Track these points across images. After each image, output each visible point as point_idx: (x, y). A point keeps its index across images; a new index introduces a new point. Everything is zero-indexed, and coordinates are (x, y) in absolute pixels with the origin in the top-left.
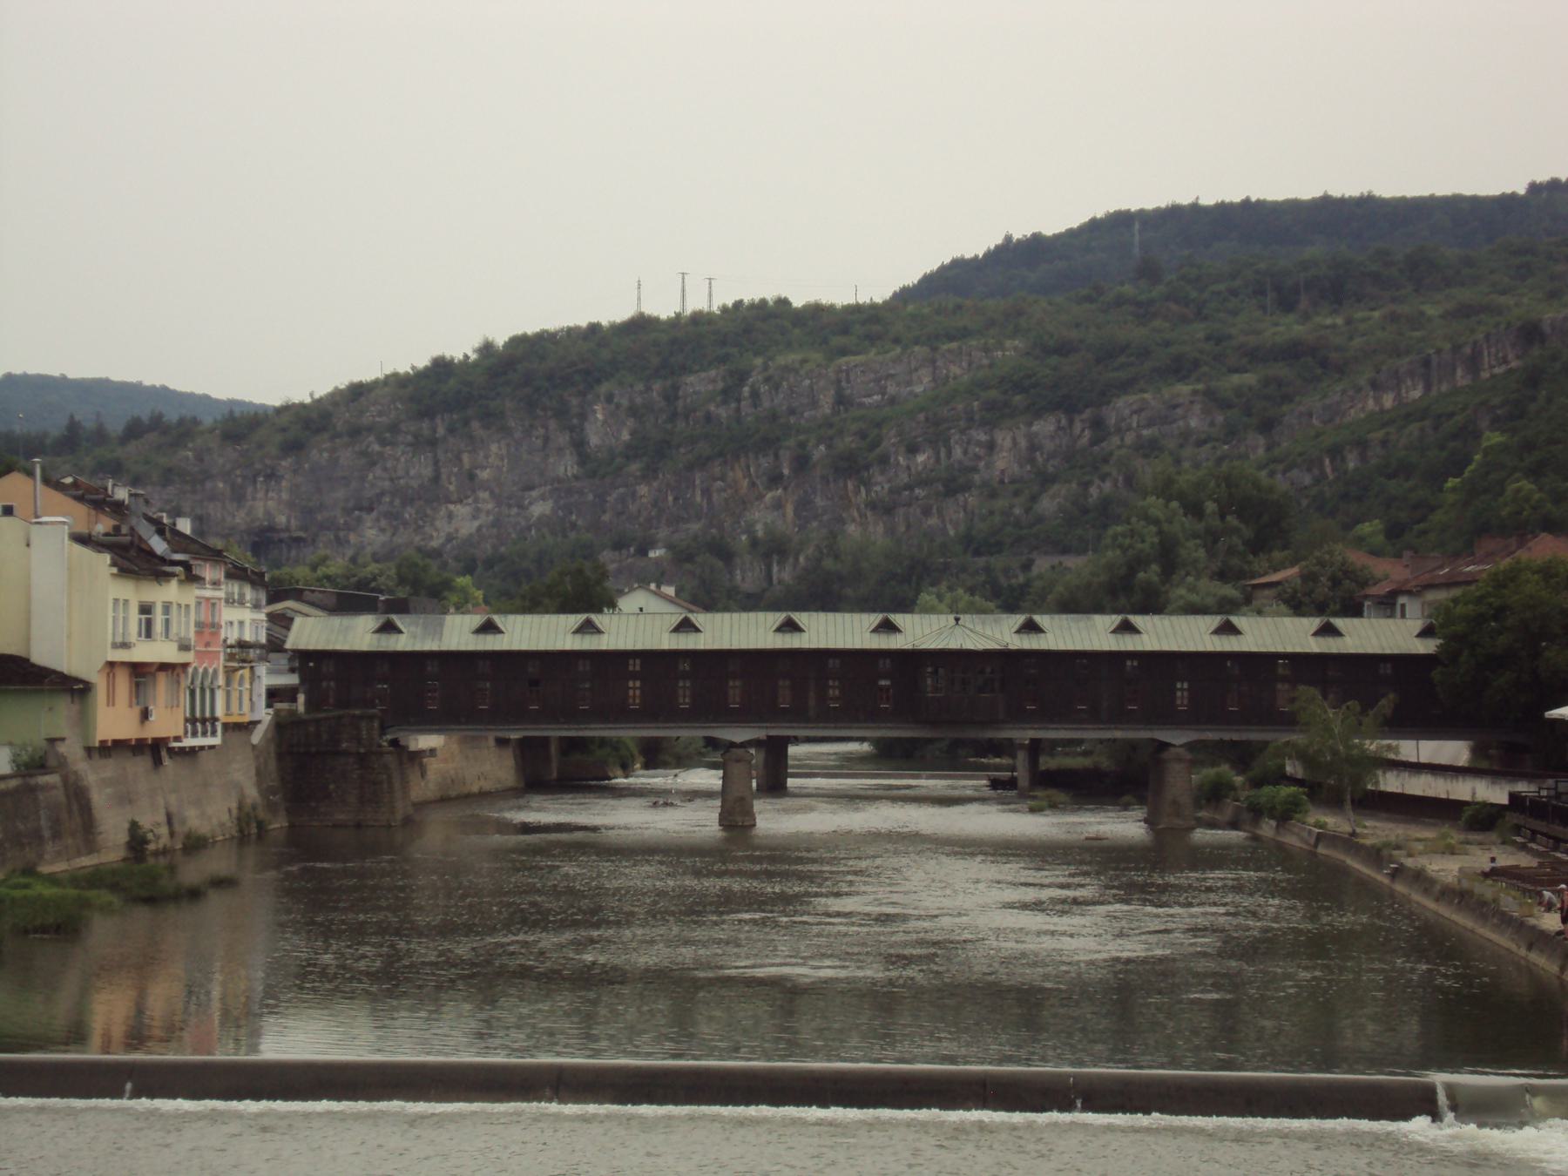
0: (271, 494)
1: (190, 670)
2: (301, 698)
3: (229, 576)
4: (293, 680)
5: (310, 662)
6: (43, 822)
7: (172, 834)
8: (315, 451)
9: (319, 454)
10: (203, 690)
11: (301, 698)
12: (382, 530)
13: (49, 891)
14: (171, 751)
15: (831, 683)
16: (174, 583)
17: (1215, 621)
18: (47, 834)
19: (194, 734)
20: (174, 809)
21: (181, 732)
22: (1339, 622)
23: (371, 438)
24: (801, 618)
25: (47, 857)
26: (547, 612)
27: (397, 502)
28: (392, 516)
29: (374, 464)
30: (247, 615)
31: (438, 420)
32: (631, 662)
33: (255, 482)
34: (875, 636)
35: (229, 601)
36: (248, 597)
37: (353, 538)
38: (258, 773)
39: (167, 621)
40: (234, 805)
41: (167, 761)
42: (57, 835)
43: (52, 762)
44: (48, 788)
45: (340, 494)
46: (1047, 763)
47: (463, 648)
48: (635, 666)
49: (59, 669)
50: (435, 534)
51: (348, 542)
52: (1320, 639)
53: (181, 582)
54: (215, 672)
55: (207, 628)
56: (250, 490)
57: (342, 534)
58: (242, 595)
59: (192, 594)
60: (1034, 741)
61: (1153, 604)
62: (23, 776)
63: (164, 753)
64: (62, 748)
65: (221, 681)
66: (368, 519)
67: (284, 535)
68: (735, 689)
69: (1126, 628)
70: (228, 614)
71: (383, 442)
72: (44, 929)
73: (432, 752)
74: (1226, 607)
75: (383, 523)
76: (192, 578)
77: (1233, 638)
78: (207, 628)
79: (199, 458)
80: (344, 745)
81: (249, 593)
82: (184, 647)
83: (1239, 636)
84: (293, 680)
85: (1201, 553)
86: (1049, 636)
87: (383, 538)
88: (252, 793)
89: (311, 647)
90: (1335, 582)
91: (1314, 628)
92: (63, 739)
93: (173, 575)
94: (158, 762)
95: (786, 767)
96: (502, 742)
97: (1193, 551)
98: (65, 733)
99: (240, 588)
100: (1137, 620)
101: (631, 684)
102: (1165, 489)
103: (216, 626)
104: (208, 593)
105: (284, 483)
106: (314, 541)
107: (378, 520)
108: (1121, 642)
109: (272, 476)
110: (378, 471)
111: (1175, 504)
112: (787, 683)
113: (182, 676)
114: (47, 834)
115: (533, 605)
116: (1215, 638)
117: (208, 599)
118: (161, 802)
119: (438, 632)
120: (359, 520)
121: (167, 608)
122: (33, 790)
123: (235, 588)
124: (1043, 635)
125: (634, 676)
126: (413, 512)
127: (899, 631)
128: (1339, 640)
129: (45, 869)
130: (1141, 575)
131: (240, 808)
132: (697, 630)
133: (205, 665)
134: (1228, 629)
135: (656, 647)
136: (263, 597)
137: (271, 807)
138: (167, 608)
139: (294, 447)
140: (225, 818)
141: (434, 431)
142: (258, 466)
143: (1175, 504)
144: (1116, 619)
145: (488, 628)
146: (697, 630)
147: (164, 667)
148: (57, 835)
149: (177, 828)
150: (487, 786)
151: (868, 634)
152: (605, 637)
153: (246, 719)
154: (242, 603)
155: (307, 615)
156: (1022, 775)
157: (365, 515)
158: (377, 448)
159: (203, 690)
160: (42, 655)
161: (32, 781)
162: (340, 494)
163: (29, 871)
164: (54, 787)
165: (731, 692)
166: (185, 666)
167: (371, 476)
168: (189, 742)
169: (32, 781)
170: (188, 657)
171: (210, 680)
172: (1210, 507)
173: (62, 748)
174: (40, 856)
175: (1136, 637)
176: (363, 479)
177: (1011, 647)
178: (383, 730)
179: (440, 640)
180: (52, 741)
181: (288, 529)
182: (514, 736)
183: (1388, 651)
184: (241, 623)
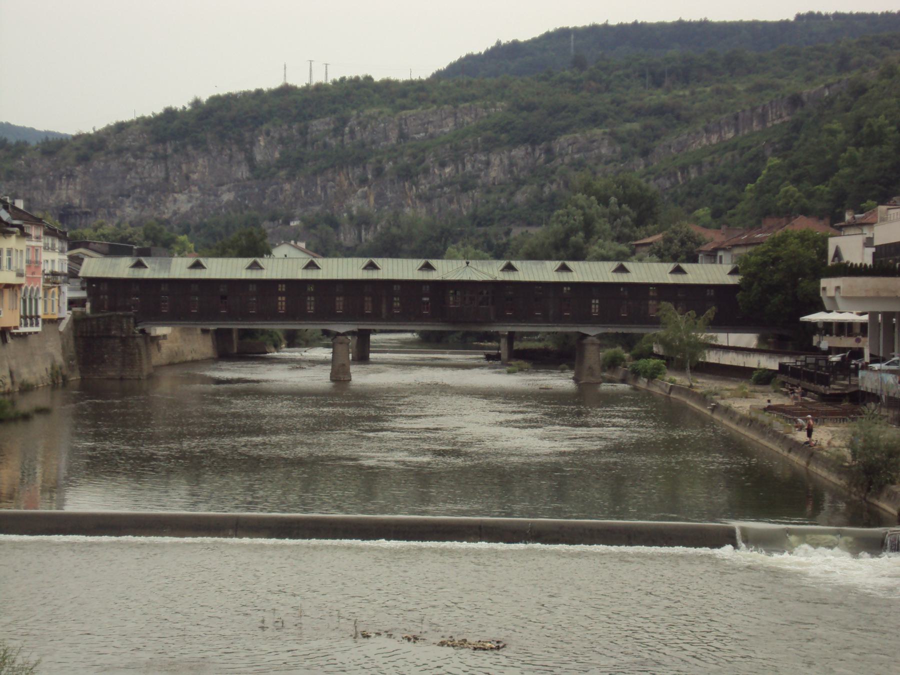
0: (70, 186)
1: (23, 288)
2: (88, 305)
3: (46, 234)
4: (83, 294)
5: (93, 284)
7: (13, 383)
8: (96, 162)
9: (98, 164)
10: (31, 300)
11: (88, 305)
12: (135, 208)
14: (12, 335)
15: (395, 299)
16: (14, 237)
17: (614, 265)
19: (26, 325)
20: (14, 369)
21: (18, 324)
22: (685, 266)
23: (129, 155)
24: (378, 261)
26: (231, 256)
27: (144, 192)
28: (142, 200)
29: (131, 169)
30: (56, 256)
31: (168, 145)
32: (280, 286)
33: (61, 179)
35: (46, 248)
36: (57, 246)
37: (118, 213)
38: (63, 348)
39: (10, 259)
40: (49, 367)
41: (10, 341)
45: (111, 187)
46: (518, 345)
47: (182, 277)
48: (282, 288)
50: (166, 211)
51: (115, 214)
52: (674, 276)
53: (17, 237)
54: (38, 289)
55: (33, 264)
56: (58, 184)
57: (112, 210)
58: (53, 245)
59: (24, 244)
60: (510, 333)
61: (579, 255)
63: (8, 336)
65: (41, 294)
66: (127, 202)
67: (78, 211)
68: (340, 301)
69: (564, 268)
70: (45, 256)
71: (136, 157)
73: (165, 337)
74: (621, 256)
75: (136, 204)
76: (24, 234)
78: (33, 264)
79: (28, 165)
80: (113, 333)
81: (58, 244)
82: (20, 275)
83: (628, 274)
84: (83, 294)
85: (608, 226)
86: (520, 273)
87: (136, 213)
88: (60, 360)
89: (94, 275)
90: (683, 243)
91: (670, 269)
93: (13, 233)
94: (5, 341)
95: (369, 347)
96: (205, 331)
97: (602, 225)
99: (52, 240)
100: (571, 264)
101: (280, 299)
102: (587, 189)
103: (38, 263)
104: (34, 243)
105: (78, 180)
106: (95, 214)
107: (133, 202)
109: (71, 176)
110: (133, 174)
111: (593, 198)
112: (370, 299)
113: (19, 292)
115: (223, 252)
116: (615, 275)
117: (33, 247)
118: (6, 364)
119: (168, 267)
120: (122, 202)
121: (9, 252)
123: (49, 240)
124: (516, 272)
125: (282, 294)
126: (153, 198)
127: (435, 269)
128: (684, 276)
130: (573, 238)
131: (53, 368)
132: (318, 268)
133: (32, 285)
134: (622, 269)
136: (66, 246)
137: (71, 368)
138: (9, 252)
139: (84, 159)
140: (44, 373)
141: (165, 150)
142: (63, 170)
143: (593, 198)
144: (558, 264)
145: (197, 265)
146: (318, 268)
147: (8, 286)
149: (16, 379)
150: (196, 356)
151: (416, 271)
152: (265, 272)
153: (56, 317)
154: (53, 249)
155: (91, 257)
156: (504, 352)
157: (125, 199)
158: (132, 160)
159: (31, 300)
162: (111, 187)
165: (337, 304)
166: (20, 286)
167: (128, 177)
168: (23, 330)
170: (22, 281)
171: (35, 294)
172: (613, 200)
175: (570, 273)
176: (124, 178)
177: (498, 279)
178: (136, 324)
179: (169, 272)
181: (80, 207)
182: (212, 328)
183: (712, 283)
184: (53, 261)
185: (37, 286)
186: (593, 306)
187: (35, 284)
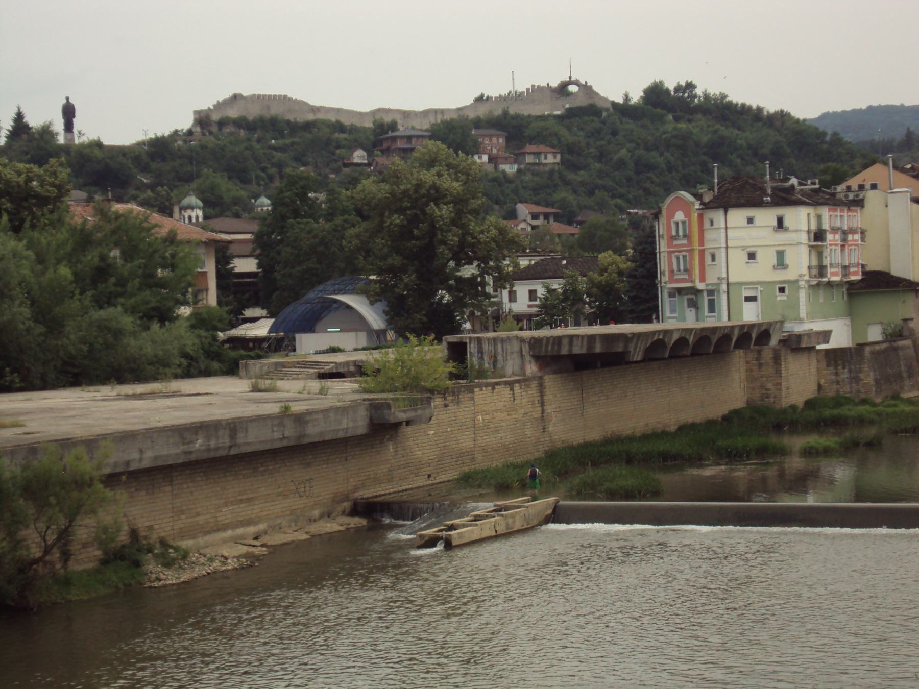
6: (903, 368)
13: (908, 409)
18: (905, 375)
25: (906, 388)
42: (910, 376)
43: (906, 333)
44: (903, 348)
49: (908, 278)
62: (890, 342)
64: (911, 325)
72: (906, 431)
92: (912, 319)
98: (913, 316)
114: (905, 375)
122: (895, 349)
129: (905, 395)
148: (910, 376)
160: (897, 271)
161: (895, 344)
163: (896, 397)
164: (908, 347)
169: (895, 344)
173: (911, 325)
174: (902, 388)
180: (905, 320)
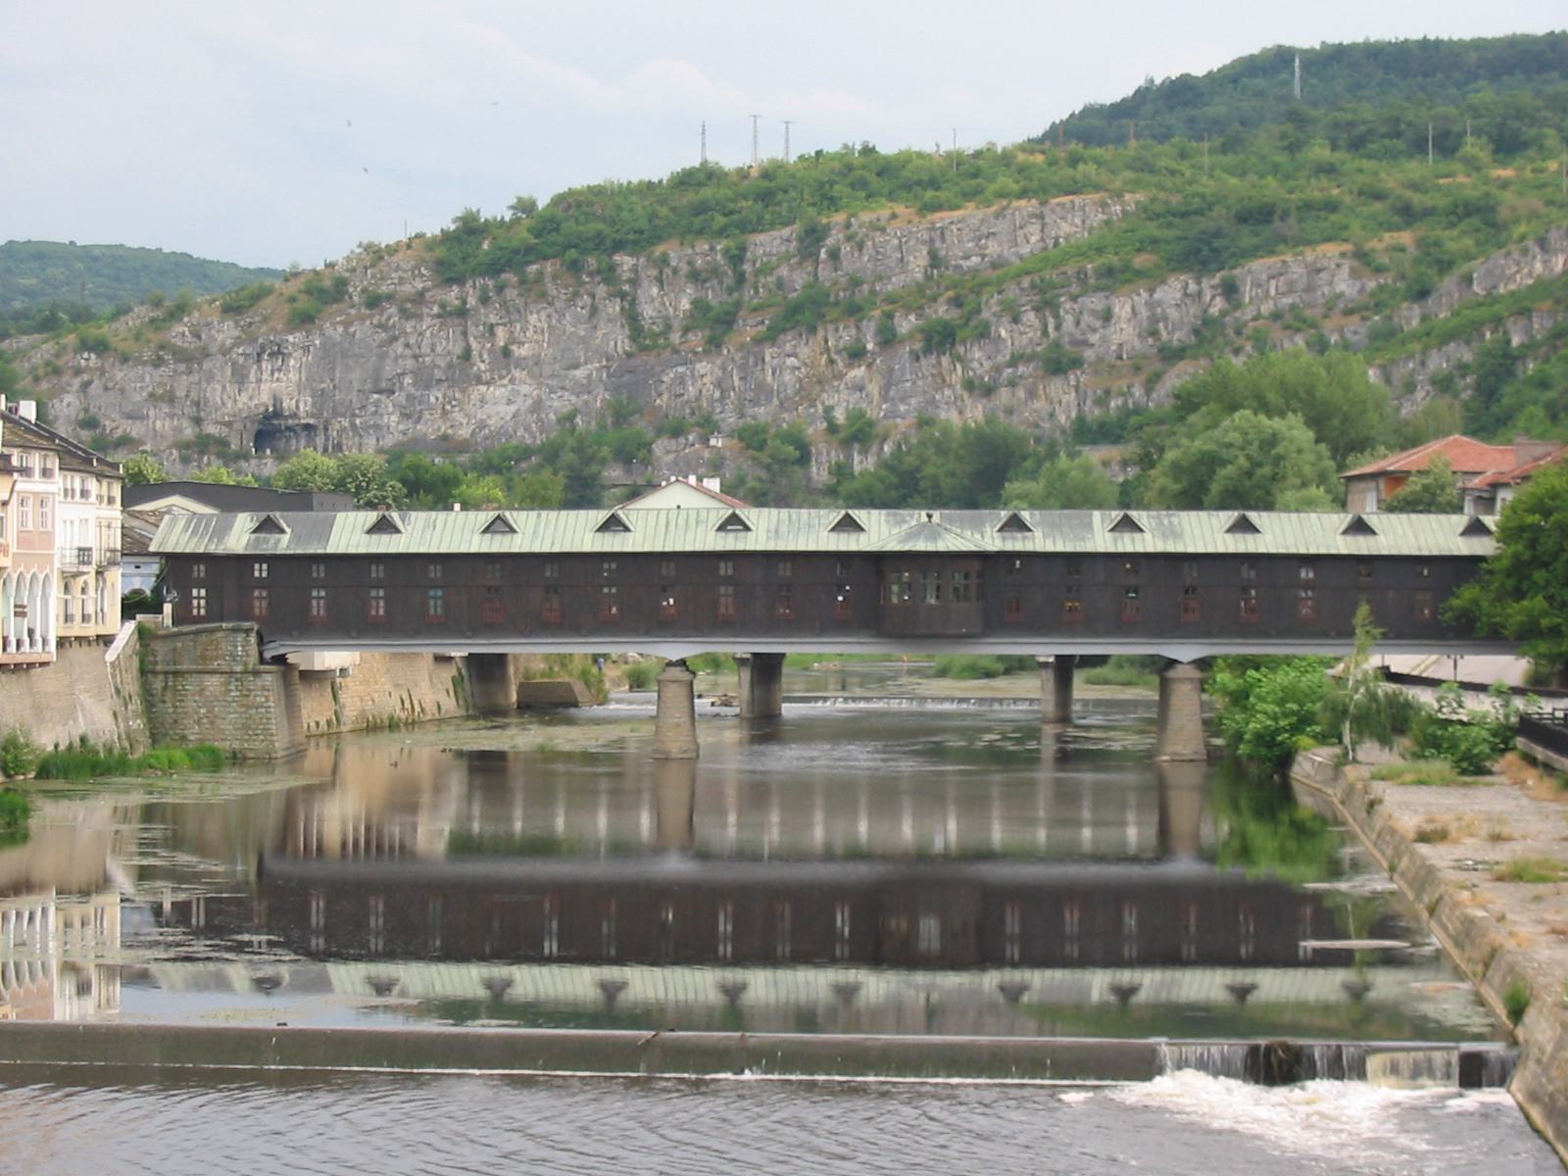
5: (177, 567)
32: (257, 566)
34: (834, 535)
47: (352, 550)
52: (1350, 538)
77: (1249, 537)
81: (92, 485)
83: (1257, 535)
86: (1038, 533)
108: (1119, 543)
112: (731, 590)
116: (1229, 537)
117: (35, 494)
119: (325, 535)
127: (862, 529)
128: (1370, 539)
135: (576, 548)
145: (383, 526)
152: (517, 538)
175: (1137, 536)
183: (1425, 553)
185: (47, 571)
186: (314, 603)
187: (41, 568)
